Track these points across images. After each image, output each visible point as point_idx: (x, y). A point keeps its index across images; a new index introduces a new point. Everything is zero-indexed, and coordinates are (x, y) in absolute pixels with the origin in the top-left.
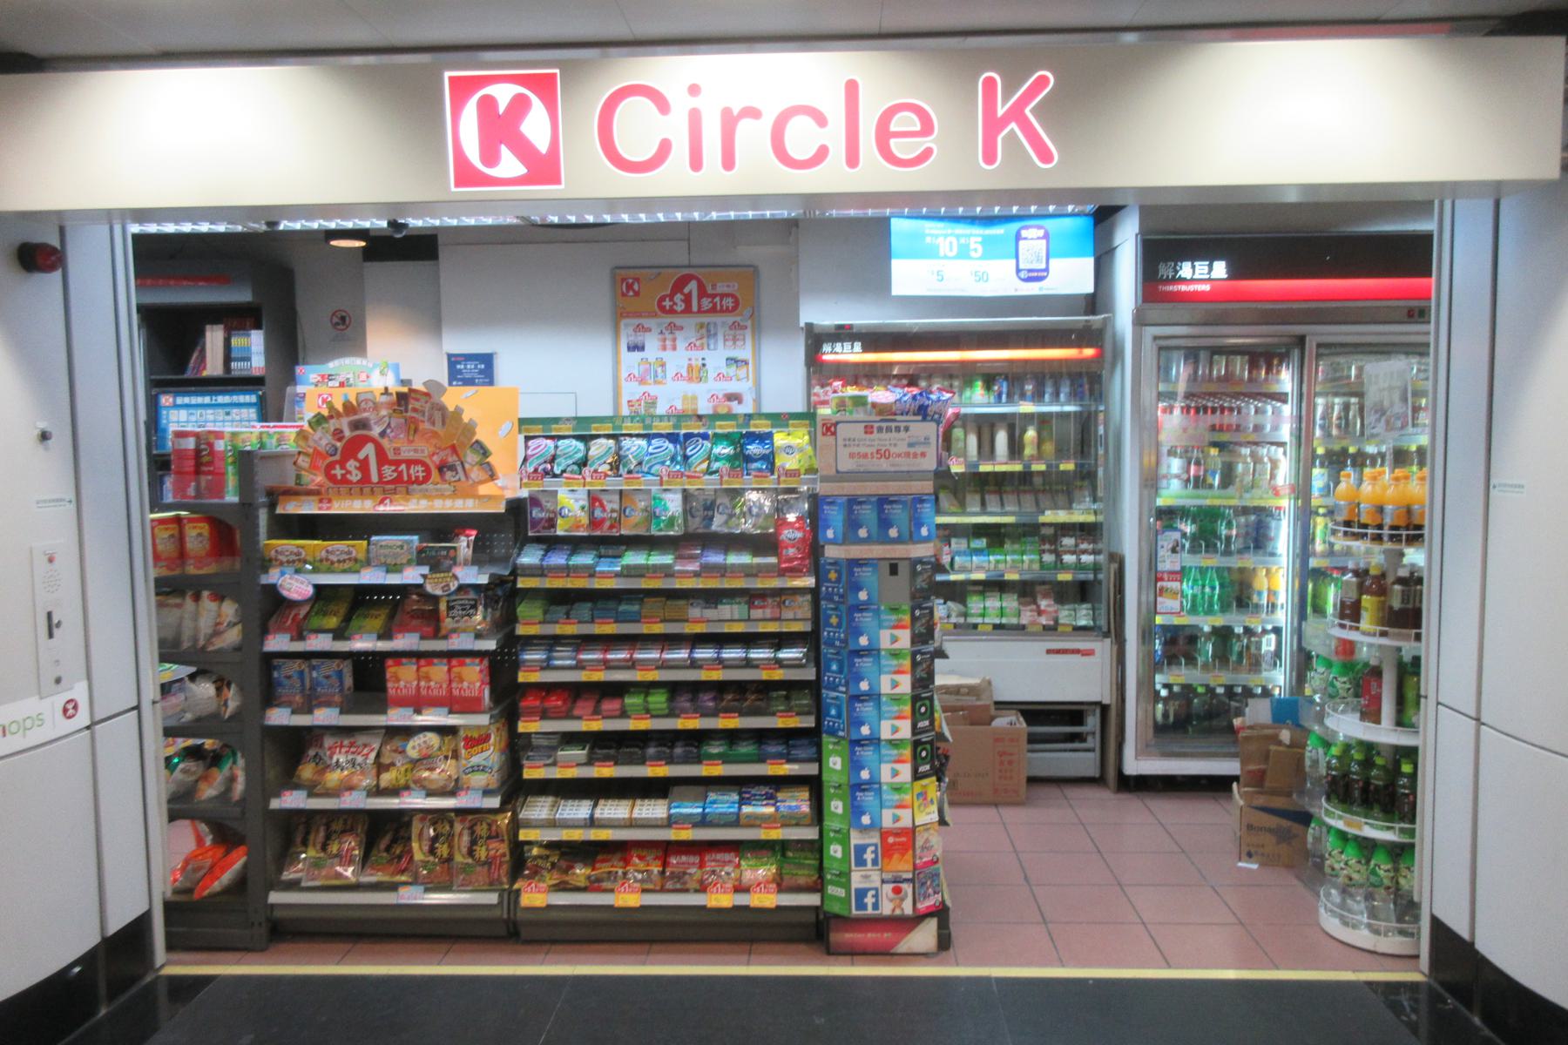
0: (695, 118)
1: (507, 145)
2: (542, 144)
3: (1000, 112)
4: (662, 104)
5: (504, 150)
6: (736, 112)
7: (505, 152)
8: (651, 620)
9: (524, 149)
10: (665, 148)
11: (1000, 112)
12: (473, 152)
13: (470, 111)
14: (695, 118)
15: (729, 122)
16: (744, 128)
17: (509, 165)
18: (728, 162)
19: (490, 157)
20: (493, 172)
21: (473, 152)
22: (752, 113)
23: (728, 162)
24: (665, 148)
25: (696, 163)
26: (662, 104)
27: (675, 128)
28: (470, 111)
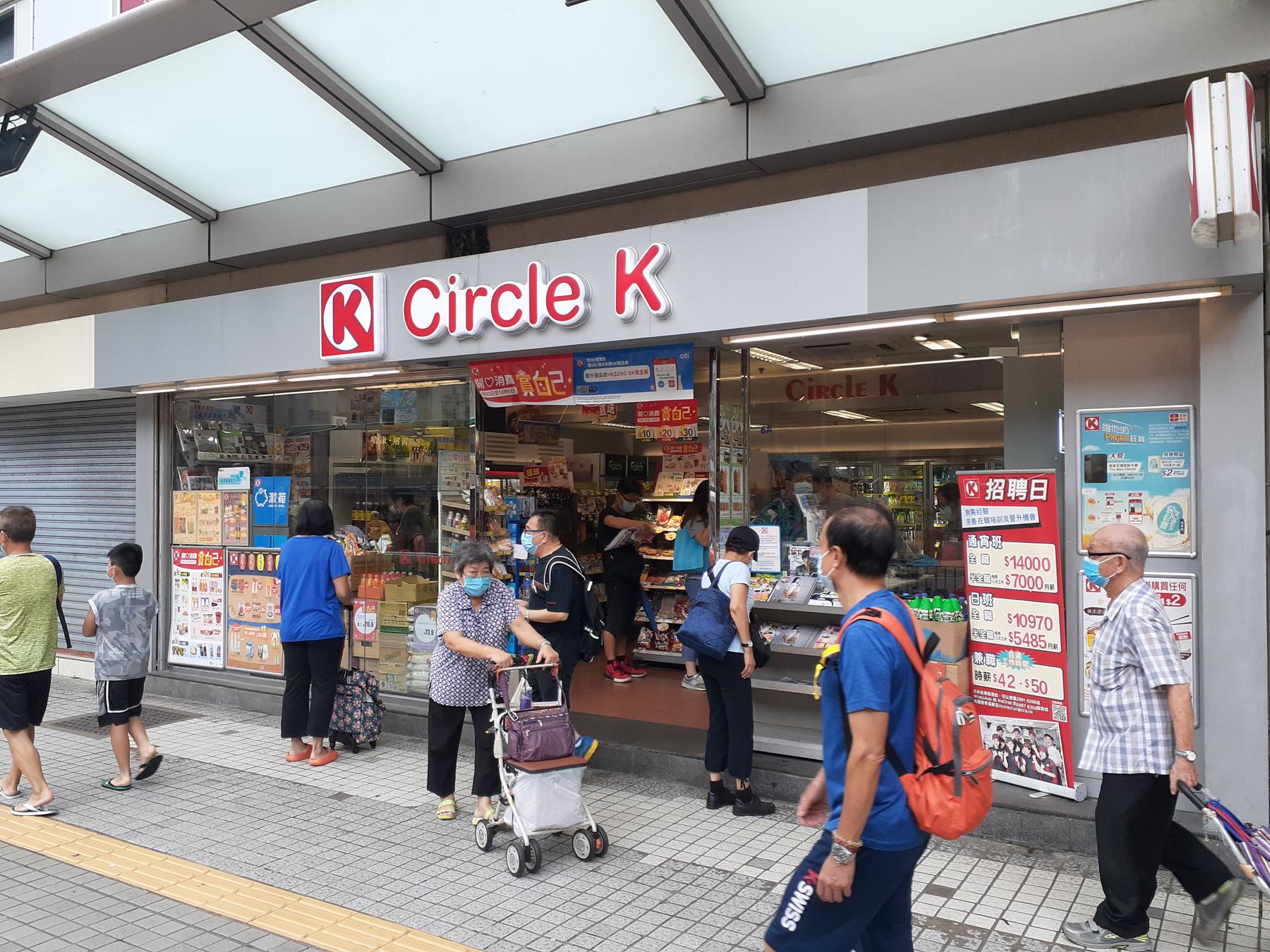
0: (452, 297)
2: (367, 329)
5: (347, 333)
6: (474, 290)
7: (347, 333)
14: (452, 297)
15: (470, 299)
17: (349, 342)
19: (339, 337)
20: (340, 347)
22: (482, 292)
27: (442, 305)
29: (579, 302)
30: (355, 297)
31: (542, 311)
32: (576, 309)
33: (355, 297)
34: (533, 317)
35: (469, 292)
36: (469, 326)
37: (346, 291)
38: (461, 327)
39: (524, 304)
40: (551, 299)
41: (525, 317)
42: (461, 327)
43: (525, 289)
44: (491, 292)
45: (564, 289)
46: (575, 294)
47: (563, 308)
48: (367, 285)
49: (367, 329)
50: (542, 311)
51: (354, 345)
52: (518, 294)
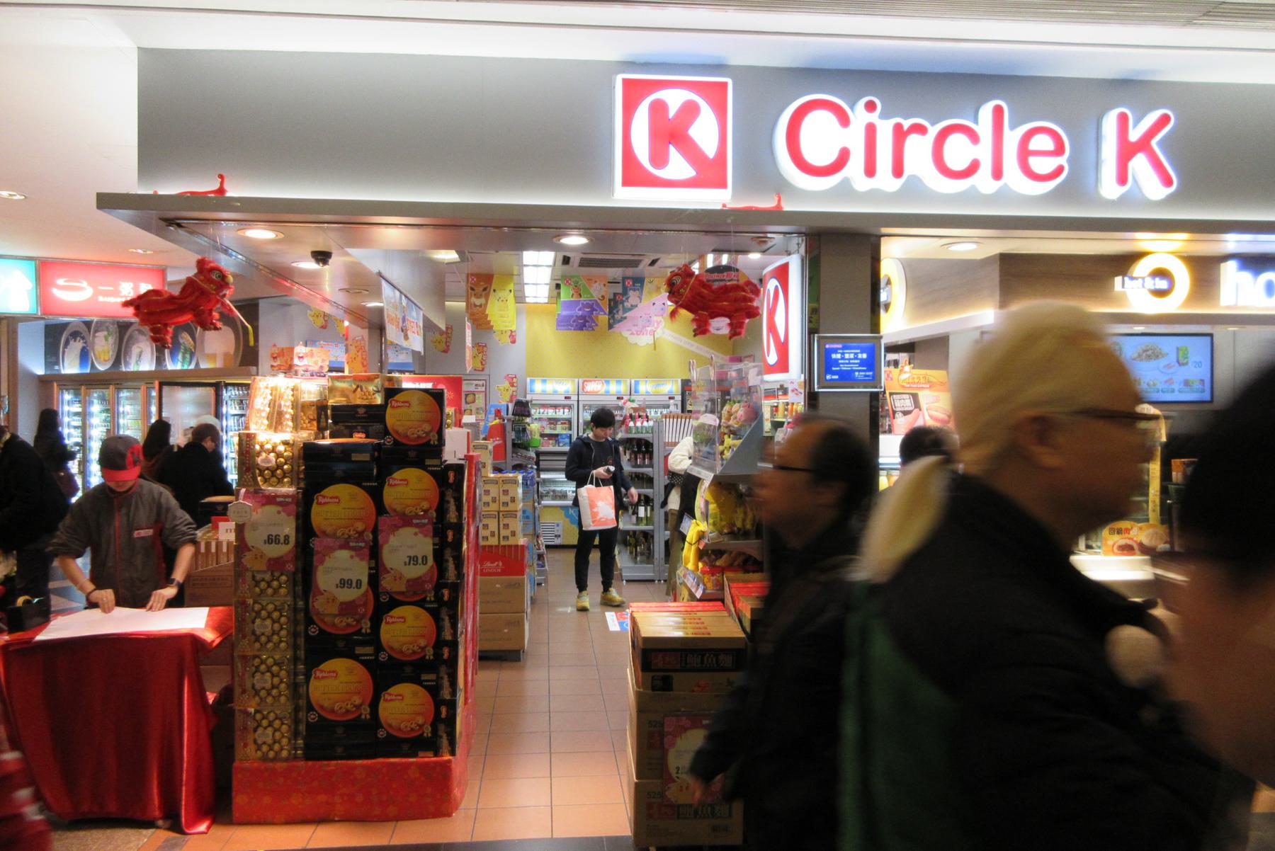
0: (871, 130)
6: (906, 124)
13: (642, 116)
14: (871, 130)
15: (900, 135)
16: (912, 141)
18: (898, 171)
22: (920, 129)
23: (898, 171)
25: (870, 170)
28: (642, 116)
29: (1062, 160)
30: (690, 111)
32: (1059, 170)
33: (690, 111)
35: (898, 127)
37: (674, 99)
39: (983, 151)
40: (1024, 153)
45: (1042, 142)
46: (1059, 150)
47: (1041, 165)
52: (974, 137)
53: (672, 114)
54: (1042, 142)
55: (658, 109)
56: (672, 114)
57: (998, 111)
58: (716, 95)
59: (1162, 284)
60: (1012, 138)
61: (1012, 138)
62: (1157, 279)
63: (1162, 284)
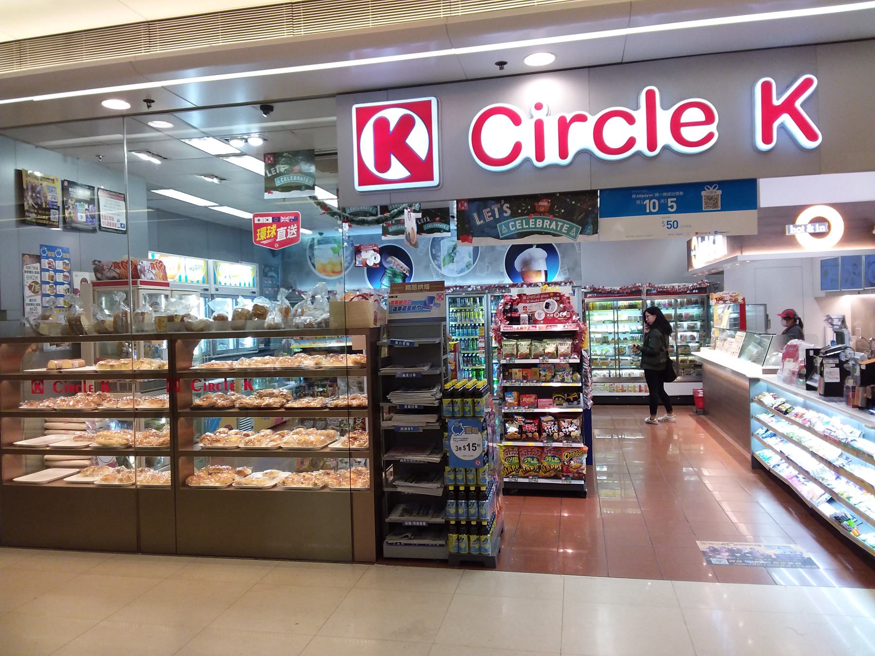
1: (394, 155)
2: (423, 155)
3: (776, 102)
4: (516, 120)
5: (394, 160)
7: (394, 160)
8: (550, 406)
9: (408, 158)
10: (517, 148)
11: (776, 102)
12: (370, 162)
15: (564, 126)
17: (397, 170)
19: (383, 164)
21: (370, 162)
22: (581, 118)
24: (517, 148)
26: (516, 120)
31: (664, 137)
32: (710, 136)
33: (406, 125)
34: (652, 145)
36: (563, 153)
37: (393, 116)
38: (552, 156)
39: (639, 131)
40: (676, 126)
41: (641, 145)
42: (552, 156)
43: (641, 115)
44: (592, 120)
48: (424, 112)
49: (423, 155)
50: (664, 137)
51: (405, 173)
52: (630, 120)
53: (392, 127)
54: (694, 114)
55: (382, 125)
56: (392, 127)
57: (650, 96)
58: (424, 112)
59: (822, 228)
60: (664, 118)
61: (664, 118)
62: (817, 225)
63: (822, 228)
